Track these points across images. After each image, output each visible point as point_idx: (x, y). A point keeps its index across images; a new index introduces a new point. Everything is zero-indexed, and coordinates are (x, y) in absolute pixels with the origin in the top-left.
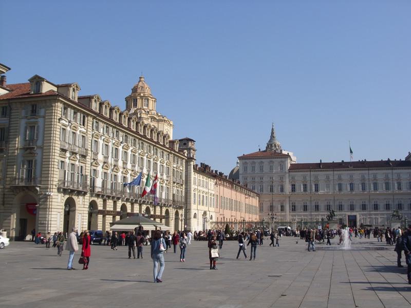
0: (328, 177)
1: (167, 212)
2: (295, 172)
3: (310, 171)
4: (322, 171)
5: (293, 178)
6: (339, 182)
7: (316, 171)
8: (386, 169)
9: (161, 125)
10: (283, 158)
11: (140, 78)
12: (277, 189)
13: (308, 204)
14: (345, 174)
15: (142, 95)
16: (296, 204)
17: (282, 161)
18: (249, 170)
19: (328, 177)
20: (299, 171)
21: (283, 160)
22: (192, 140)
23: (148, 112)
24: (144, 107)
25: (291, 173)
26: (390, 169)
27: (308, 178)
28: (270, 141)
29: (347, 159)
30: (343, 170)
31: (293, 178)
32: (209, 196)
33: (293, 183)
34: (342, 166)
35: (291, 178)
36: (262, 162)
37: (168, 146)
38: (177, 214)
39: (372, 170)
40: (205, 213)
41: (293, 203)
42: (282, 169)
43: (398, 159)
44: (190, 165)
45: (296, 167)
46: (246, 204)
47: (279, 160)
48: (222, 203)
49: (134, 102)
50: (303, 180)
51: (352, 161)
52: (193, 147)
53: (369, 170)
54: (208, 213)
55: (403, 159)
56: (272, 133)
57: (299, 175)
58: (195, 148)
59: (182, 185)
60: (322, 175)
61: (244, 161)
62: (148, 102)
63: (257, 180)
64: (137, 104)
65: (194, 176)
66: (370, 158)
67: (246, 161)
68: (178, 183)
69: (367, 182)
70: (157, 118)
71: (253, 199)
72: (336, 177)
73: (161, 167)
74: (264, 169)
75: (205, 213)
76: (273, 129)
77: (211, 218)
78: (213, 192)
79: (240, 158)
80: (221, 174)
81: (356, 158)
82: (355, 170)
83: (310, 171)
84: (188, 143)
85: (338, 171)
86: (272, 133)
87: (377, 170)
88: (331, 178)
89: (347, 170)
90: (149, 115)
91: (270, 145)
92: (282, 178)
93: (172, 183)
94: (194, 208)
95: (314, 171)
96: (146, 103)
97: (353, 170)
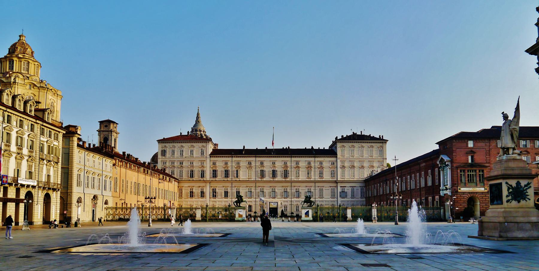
0: (250, 163)
1: (29, 195)
4: (244, 157)
5: (214, 164)
6: (261, 169)
8: (309, 157)
9: (42, 93)
11: (20, 36)
12: (197, 176)
13: (229, 191)
14: (267, 161)
15: (20, 56)
16: (217, 191)
17: (203, 146)
19: (250, 163)
21: (204, 144)
22: (114, 122)
23: (28, 77)
24: (22, 72)
25: (212, 159)
26: (313, 157)
27: (229, 164)
28: (195, 126)
29: (270, 147)
31: (214, 164)
32: (104, 178)
33: (214, 169)
35: (212, 163)
36: (182, 146)
37: (33, 114)
38: (47, 199)
39: (295, 157)
40: (95, 197)
41: (213, 190)
42: (202, 153)
43: (322, 148)
44: (73, 141)
45: (217, 152)
46: (159, 189)
47: (200, 144)
48: (118, 185)
49: (10, 64)
50: (224, 166)
52: (115, 129)
54: (100, 198)
56: (198, 117)
57: (220, 161)
58: (118, 131)
59: (57, 163)
60: (244, 161)
61: (164, 144)
62: (28, 66)
63: (176, 164)
64: (13, 67)
65: (78, 155)
66: (294, 146)
68: (49, 161)
69: (289, 169)
70: (39, 85)
71: (170, 183)
72: (258, 164)
73: (19, 139)
74: (184, 154)
75: (95, 197)
76: (198, 114)
77: (106, 203)
78: (111, 175)
79: (160, 141)
80: (129, 155)
81: (278, 146)
84: (110, 124)
85: (260, 157)
86: (198, 117)
87: (299, 157)
88: (253, 164)
89: (270, 157)
90: (26, 81)
91: (195, 129)
92: (202, 162)
93: (38, 160)
94: (76, 192)
95: (237, 157)
96: (26, 66)
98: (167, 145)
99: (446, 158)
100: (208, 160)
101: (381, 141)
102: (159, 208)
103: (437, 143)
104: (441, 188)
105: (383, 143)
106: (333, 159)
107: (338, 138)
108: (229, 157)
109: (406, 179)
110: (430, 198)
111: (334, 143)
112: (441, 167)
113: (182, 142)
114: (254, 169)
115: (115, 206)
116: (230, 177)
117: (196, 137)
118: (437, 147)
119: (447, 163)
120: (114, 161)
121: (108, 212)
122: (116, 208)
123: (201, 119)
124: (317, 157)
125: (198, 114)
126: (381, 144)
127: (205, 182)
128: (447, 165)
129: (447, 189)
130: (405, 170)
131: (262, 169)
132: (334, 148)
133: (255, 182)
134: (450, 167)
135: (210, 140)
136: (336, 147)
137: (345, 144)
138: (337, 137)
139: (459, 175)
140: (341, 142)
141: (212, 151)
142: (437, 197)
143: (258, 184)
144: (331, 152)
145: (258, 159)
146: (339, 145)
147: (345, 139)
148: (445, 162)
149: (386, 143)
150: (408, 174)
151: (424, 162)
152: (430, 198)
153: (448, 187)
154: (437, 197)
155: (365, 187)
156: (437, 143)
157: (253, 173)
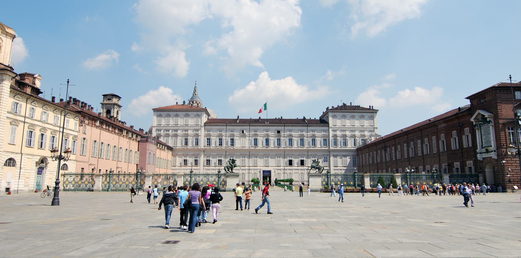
2: (211, 125)
3: (226, 126)
4: (238, 126)
7: (233, 126)
10: (199, 111)
20: (215, 125)
30: (259, 126)
34: (259, 122)
43: (313, 118)
45: (211, 122)
51: (268, 118)
53: (284, 126)
55: (318, 118)
56: (195, 91)
61: (159, 113)
67: (161, 113)
82: (271, 126)
83: (226, 126)
85: (254, 126)
86: (195, 91)
87: (292, 126)
89: (263, 126)
91: (192, 101)
95: (231, 126)
97: (269, 126)
99: (486, 114)
100: (203, 129)
101: (371, 112)
102: (129, 175)
103: (467, 98)
104: (478, 151)
105: (373, 112)
106: (326, 128)
107: (330, 108)
109: (415, 145)
110: (457, 164)
111: (325, 114)
112: (476, 125)
115: (80, 172)
116: (224, 146)
117: (191, 108)
118: (468, 103)
119: (488, 120)
120: (82, 119)
121: (65, 179)
122: (82, 175)
123: (198, 92)
124: (310, 126)
126: (372, 114)
127: (200, 150)
128: (489, 122)
129: (487, 151)
130: (413, 135)
132: (325, 118)
134: (493, 124)
135: (205, 110)
136: (328, 117)
137: (336, 114)
138: (327, 108)
139: (507, 133)
140: (332, 112)
141: (207, 120)
142: (470, 163)
144: (323, 121)
146: (330, 114)
147: (335, 110)
148: (486, 118)
149: (376, 112)
150: (418, 138)
151: (444, 123)
152: (457, 164)
153: (490, 149)
154: (470, 163)
155: (358, 155)
156: (467, 98)
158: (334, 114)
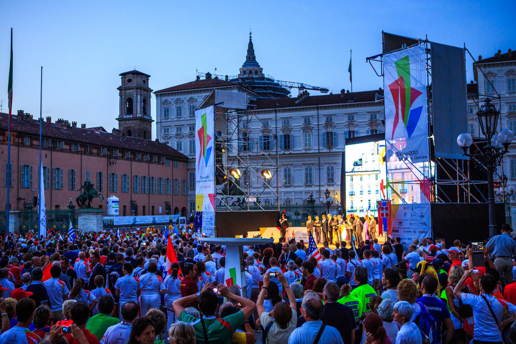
18: (173, 115)
19: (307, 120)
27: (272, 126)
34: (346, 99)
61: (164, 99)
72: (323, 121)
76: (251, 45)
85: (325, 108)
98: (169, 98)
108: (269, 112)
113: (191, 93)
114: (315, 132)
125: (251, 45)
131: (330, 130)
133: (319, 155)
143: (323, 160)
145: (322, 112)
157: (314, 139)
158: (488, 70)
